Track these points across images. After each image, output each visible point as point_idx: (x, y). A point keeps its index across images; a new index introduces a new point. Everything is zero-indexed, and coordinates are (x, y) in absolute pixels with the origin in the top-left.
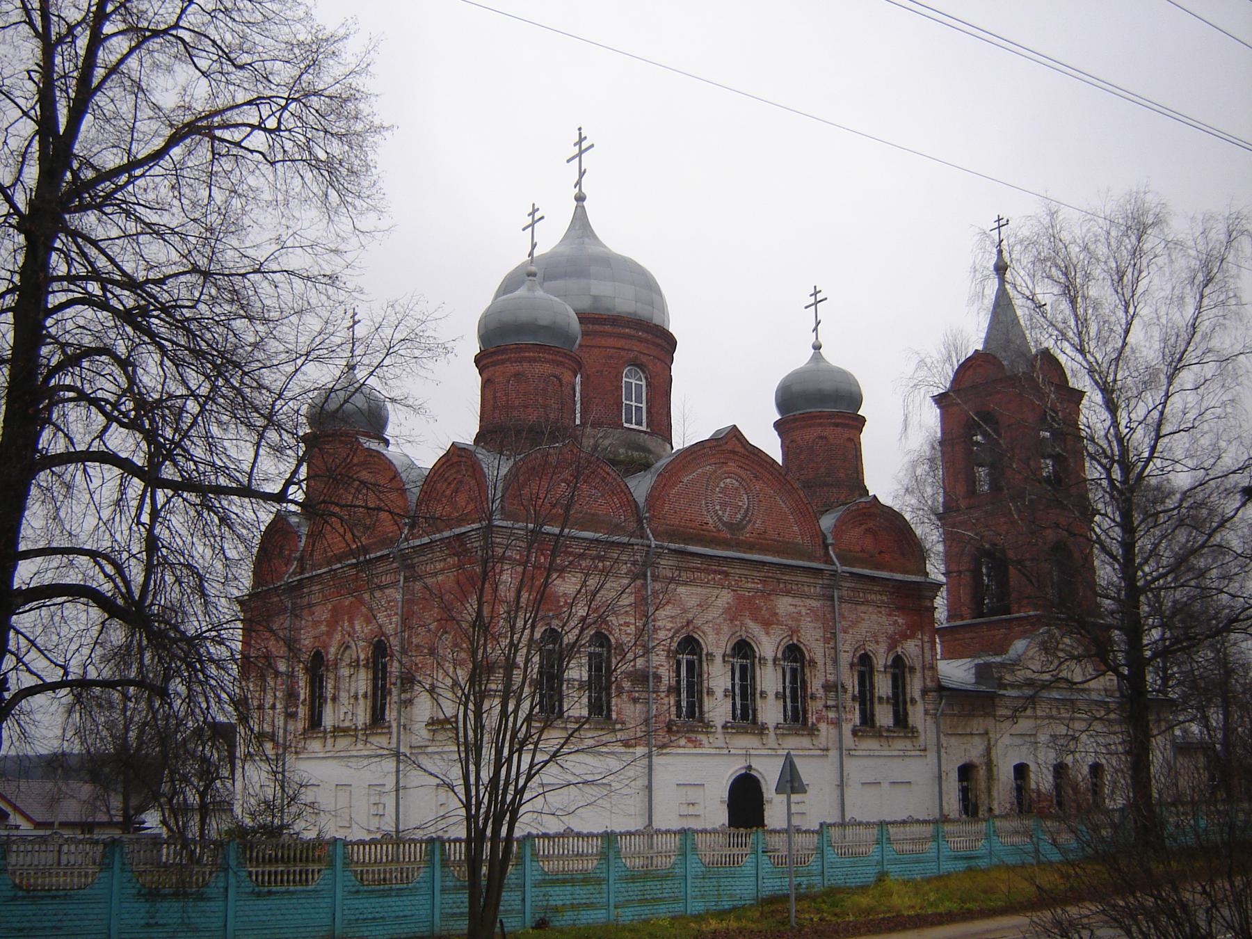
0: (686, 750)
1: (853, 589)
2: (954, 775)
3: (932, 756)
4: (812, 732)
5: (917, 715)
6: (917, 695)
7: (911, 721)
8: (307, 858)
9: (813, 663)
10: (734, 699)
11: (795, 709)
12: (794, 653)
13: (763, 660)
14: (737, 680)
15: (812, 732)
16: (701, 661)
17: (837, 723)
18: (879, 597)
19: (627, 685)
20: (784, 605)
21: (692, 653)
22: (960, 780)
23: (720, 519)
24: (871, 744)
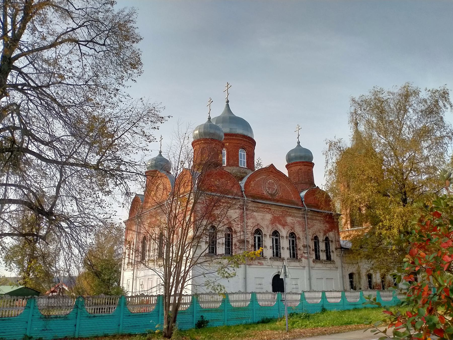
0: (258, 266)
1: (312, 215)
2: (348, 277)
3: (339, 270)
4: (300, 260)
5: (334, 256)
6: (334, 250)
7: (332, 258)
8: (110, 303)
9: (299, 238)
10: (273, 249)
11: (294, 253)
12: (292, 235)
13: (282, 237)
14: (274, 243)
15: (300, 260)
16: (262, 237)
17: (307, 258)
18: (320, 218)
19: (238, 244)
20: (289, 220)
21: (260, 234)
22: (350, 278)
23: (268, 192)
24: (319, 265)
